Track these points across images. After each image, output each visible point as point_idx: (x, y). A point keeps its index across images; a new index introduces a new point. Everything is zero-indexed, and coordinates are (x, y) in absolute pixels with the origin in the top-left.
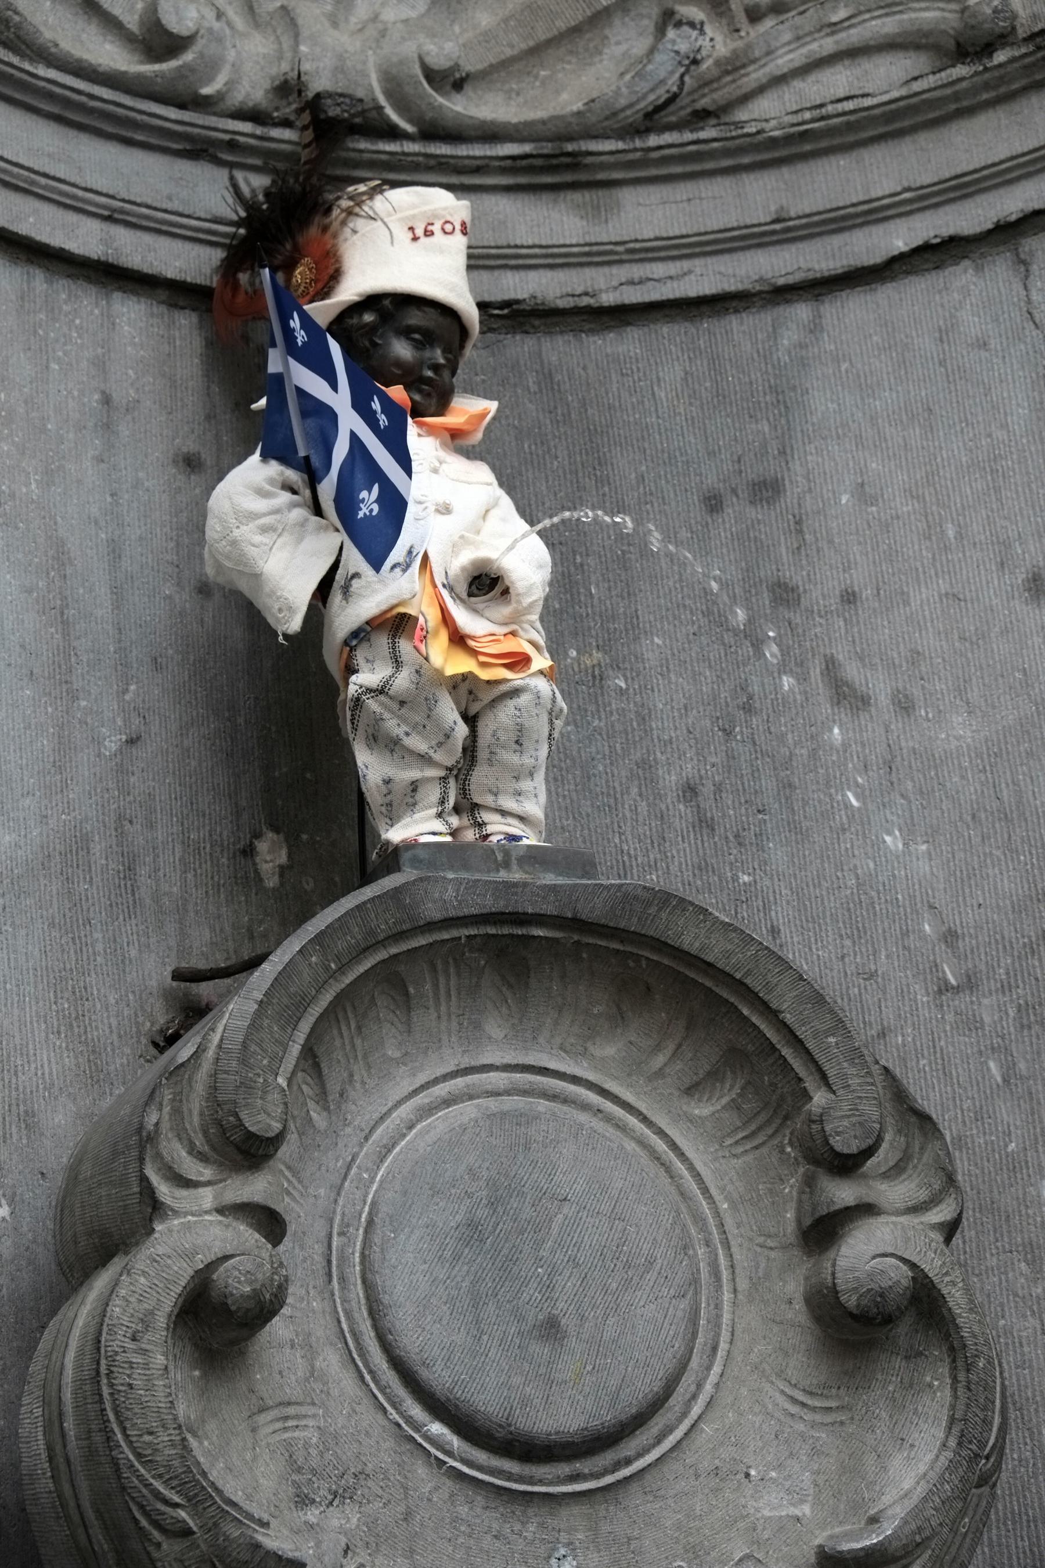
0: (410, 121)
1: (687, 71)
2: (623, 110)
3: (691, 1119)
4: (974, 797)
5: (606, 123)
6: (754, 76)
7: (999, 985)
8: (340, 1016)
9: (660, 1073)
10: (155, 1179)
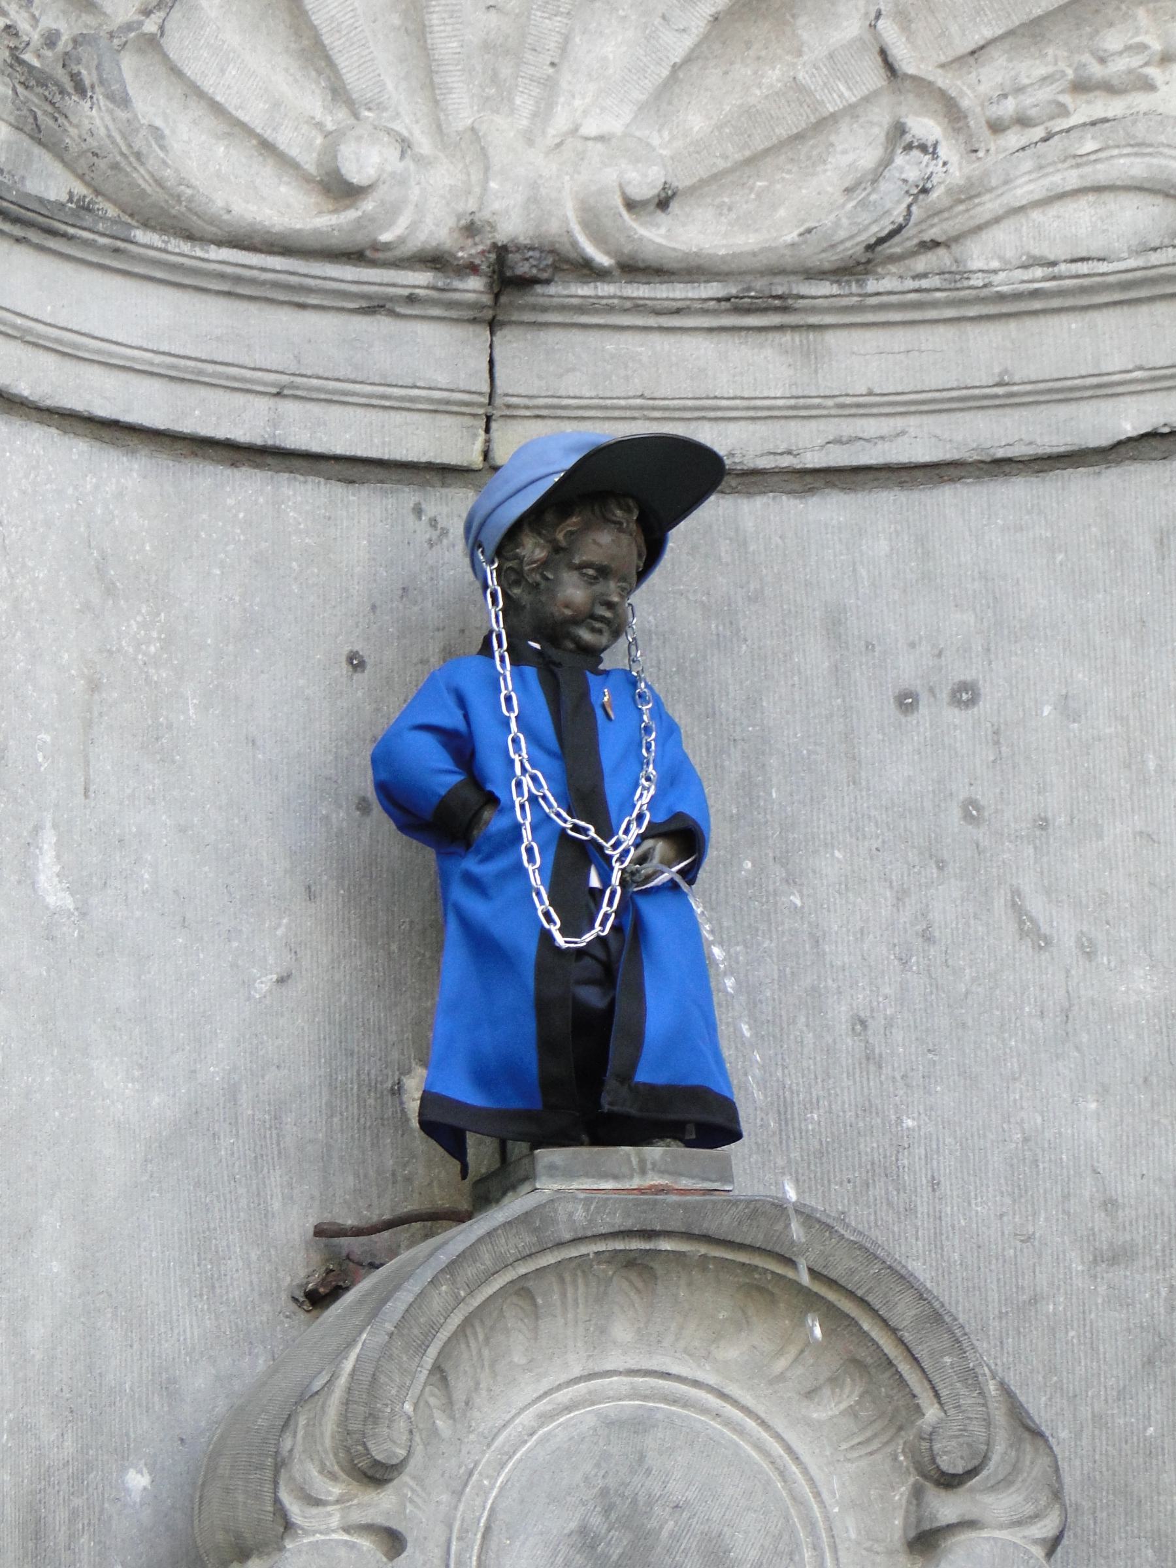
0: (608, 253)
2: (842, 242)
3: (809, 1423)
4: (1148, 1059)
5: (824, 255)
6: (989, 206)
7: (1154, 1262)
9: (781, 1377)
10: (285, 1497)
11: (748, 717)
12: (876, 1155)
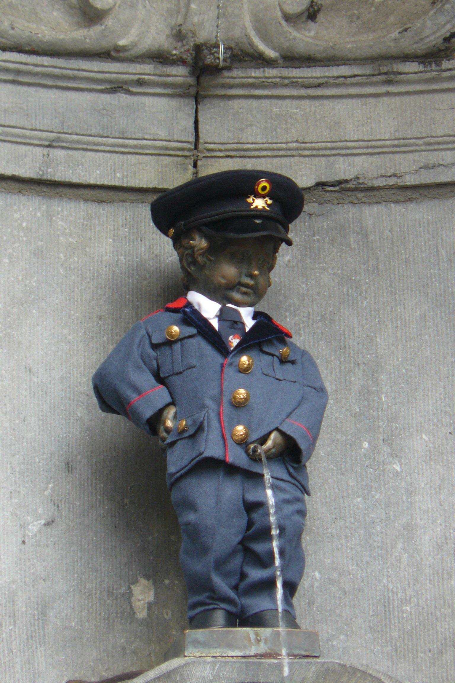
0: (273, 49)
2: (427, 37)
5: (416, 46)
11: (367, 348)
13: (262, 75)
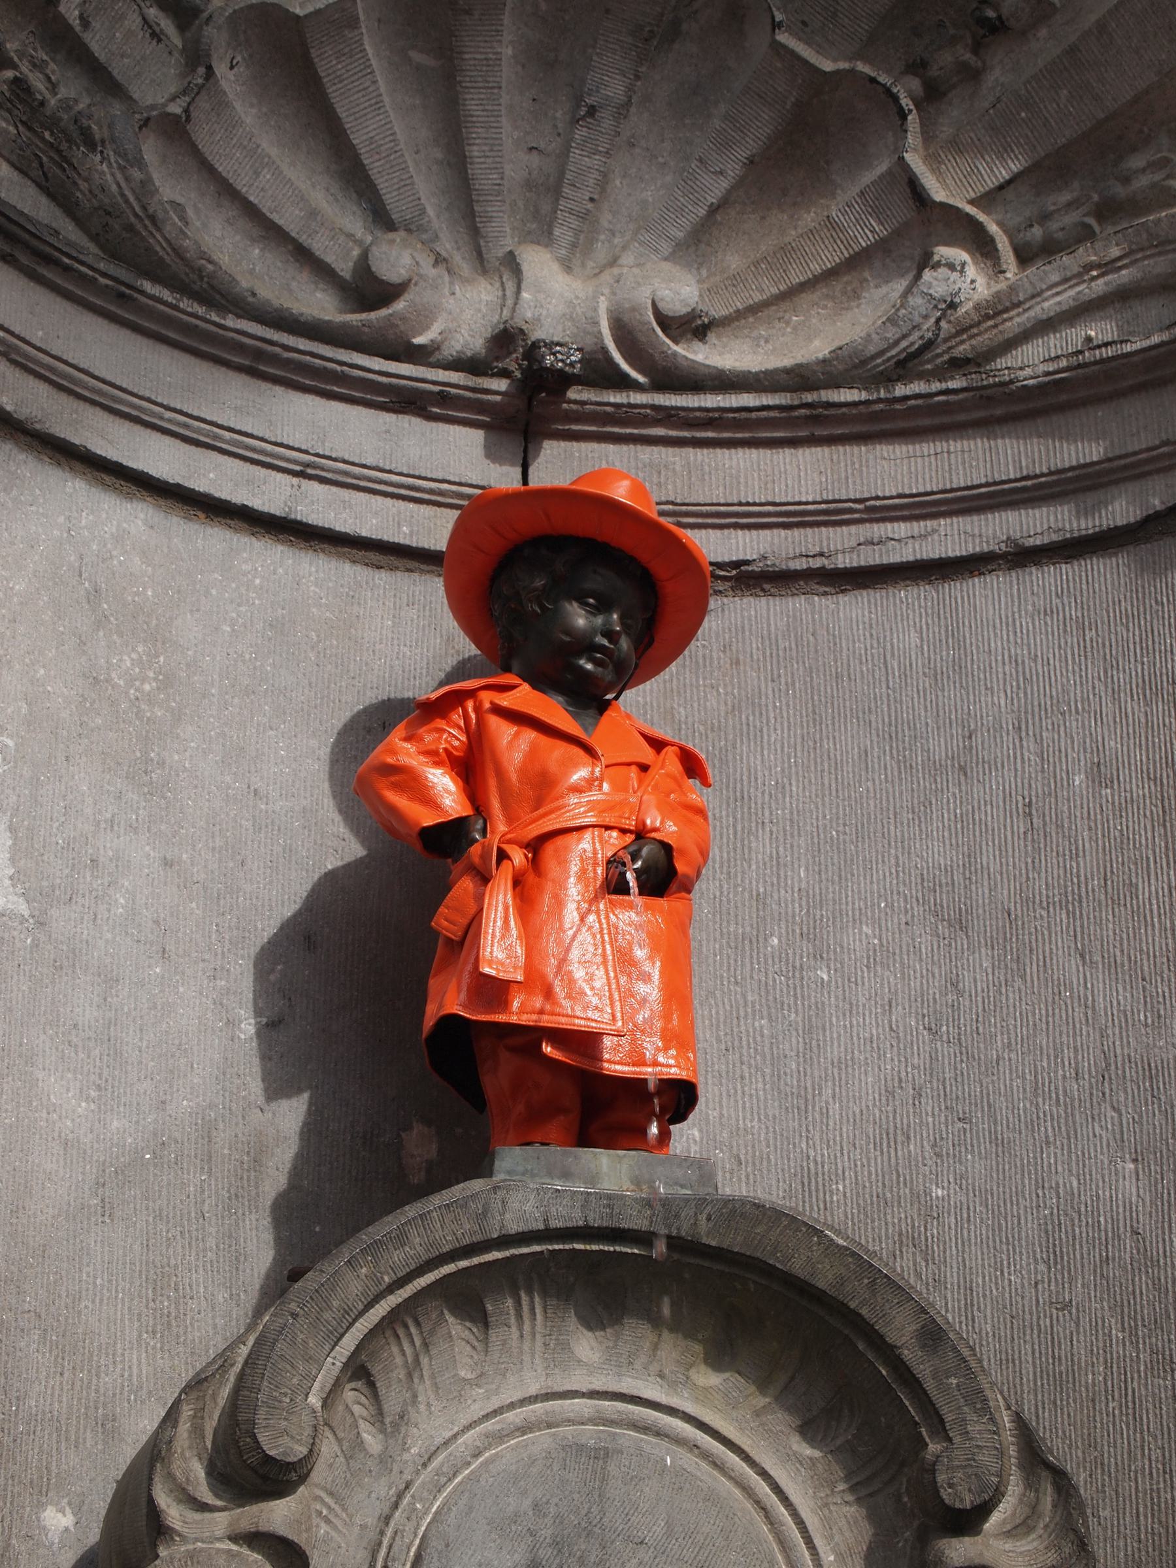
1: (944, 315)
2: (874, 357)
8: (401, 1332)
12: (904, 1226)
13: (625, 401)
